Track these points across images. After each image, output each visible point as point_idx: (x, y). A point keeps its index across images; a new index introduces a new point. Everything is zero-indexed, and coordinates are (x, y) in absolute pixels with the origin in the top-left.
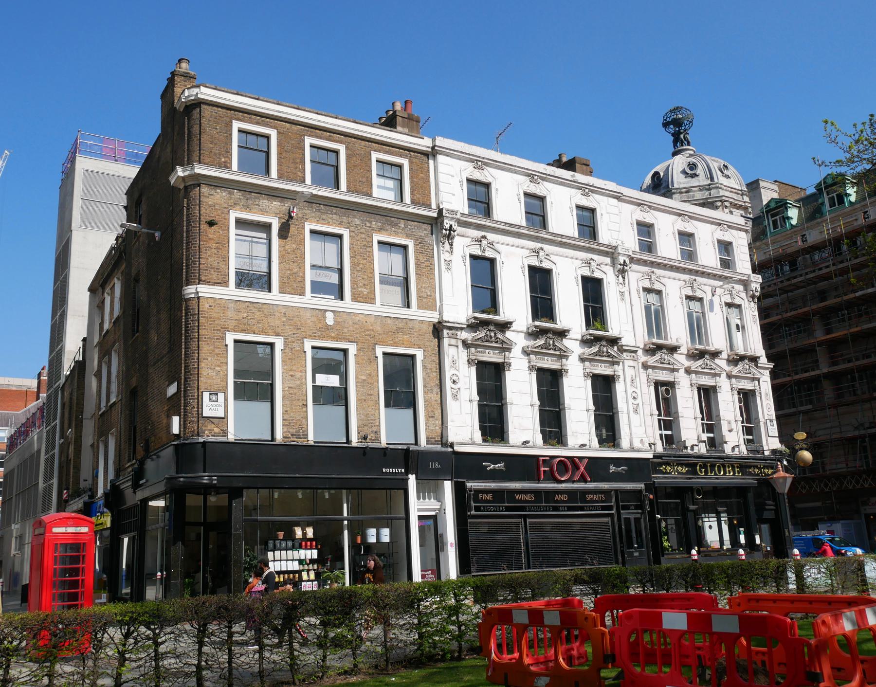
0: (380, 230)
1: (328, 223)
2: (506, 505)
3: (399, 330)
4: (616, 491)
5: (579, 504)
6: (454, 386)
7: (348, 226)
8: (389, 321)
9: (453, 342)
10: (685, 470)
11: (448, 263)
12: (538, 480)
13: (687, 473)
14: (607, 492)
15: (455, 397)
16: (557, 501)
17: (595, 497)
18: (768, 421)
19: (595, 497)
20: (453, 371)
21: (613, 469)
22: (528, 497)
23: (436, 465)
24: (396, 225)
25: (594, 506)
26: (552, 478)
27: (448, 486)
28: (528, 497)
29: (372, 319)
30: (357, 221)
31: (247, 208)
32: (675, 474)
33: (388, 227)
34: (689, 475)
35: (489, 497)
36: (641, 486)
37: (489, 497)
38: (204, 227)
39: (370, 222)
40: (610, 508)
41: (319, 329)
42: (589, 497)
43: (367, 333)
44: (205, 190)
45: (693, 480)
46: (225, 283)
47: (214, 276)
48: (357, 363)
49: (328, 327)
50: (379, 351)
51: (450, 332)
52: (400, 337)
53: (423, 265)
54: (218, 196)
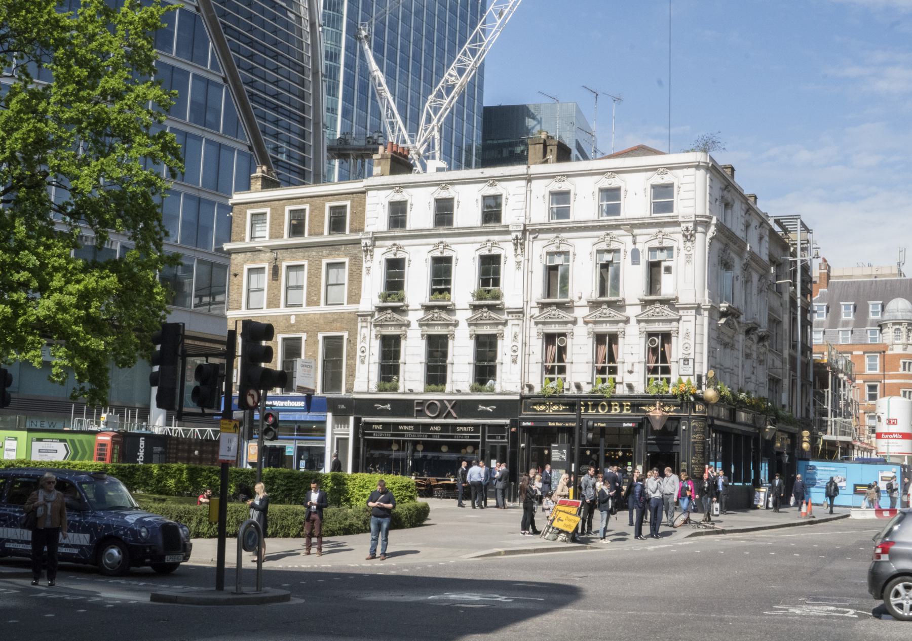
0: (328, 256)
1: (297, 259)
3: (334, 321)
4: (484, 425)
6: (362, 355)
7: (304, 258)
9: (364, 324)
10: (562, 408)
11: (368, 269)
12: (411, 416)
13: (564, 410)
14: (476, 426)
15: (363, 362)
16: (432, 431)
17: (464, 429)
18: (682, 362)
20: (363, 344)
21: (481, 407)
22: (409, 428)
23: (343, 407)
24: (339, 249)
26: (421, 413)
27: (352, 419)
28: (409, 428)
29: (318, 316)
30: (314, 253)
31: (253, 261)
33: (333, 253)
35: (380, 427)
36: (508, 421)
37: (380, 427)
38: (232, 277)
39: (322, 252)
40: (478, 437)
41: (287, 327)
42: (459, 429)
44: (233, 256)
45: (569, 417)
46: (239, 308)
47: (235, 305)
48: (307, 345)
49: (292, 325)
50: (320, 336)
51: (363, 318)
52: (334, 325)
53: (354, 274)
54: (239, 258)
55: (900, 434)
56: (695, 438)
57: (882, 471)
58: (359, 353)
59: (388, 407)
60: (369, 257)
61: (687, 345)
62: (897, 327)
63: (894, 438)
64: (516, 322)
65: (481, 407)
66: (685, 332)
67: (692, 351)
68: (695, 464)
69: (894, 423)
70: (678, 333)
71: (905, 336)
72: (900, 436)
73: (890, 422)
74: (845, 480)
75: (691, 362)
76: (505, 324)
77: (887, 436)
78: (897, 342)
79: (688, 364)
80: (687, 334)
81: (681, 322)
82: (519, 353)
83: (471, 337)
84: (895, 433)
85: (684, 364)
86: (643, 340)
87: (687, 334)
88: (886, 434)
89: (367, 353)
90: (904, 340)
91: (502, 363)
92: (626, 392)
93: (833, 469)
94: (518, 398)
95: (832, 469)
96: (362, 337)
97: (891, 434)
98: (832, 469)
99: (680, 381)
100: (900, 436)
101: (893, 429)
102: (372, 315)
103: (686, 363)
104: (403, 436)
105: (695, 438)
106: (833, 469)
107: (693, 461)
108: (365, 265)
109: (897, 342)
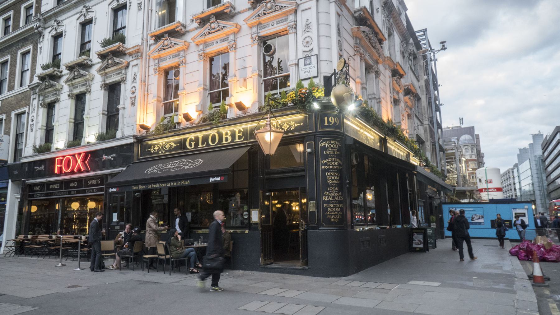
2: (45, 192)
3: (22, 99)
5: (83, 189)
8: (19, 96)
9: (34, 96)
15: (32, 130)
17: (93, 182)
18: (302, 62)
19: (93, 182)
21: (105, 157)
25: (92, 189)
29: (13, 98)
32: (162, 152)
34: (178, 150)
43: (11, 106)
55: (495, 188)
56: (326, 164)
57: (515, 209)
58: (30, 123)
59: (42, 168)
60: (41, 38)
61: (307, 39)
62: (466, 147)
63: (491, 191)
64: (135, 62)
65: (105, 157)
66: (304, 23)
67: (315, 46)
68: (328, 202)
69: (490, 182)
70: (296, 28)
71: (470, 151)
72: (495, 190)
73: (488, 182)
74: (482, 217)
75: (314, 59)
76: (127, 67)
77: (487, 190)
78: (466, 154)
79: (310, 63)
80: (308, 26)
81: (299, 13)
82: (138, 94)
83: (101, 87)
84: (492, 188)
85: (305, 65)
86: (256, 47)
87: (308, 26)
88: (486, 189)
89: (34, 122)
90: (470, 153)
91: (124, 108)
92: (240, 113)
93: (472, 209)
94: (132, 140)
95: (470, 209)
96: (33, 107)
97: (490, 189)
98: (470, 209)
99: (300, 86)
100: (495, 190)
101: (490, 186)
102: (37, 86)
103: (308, 62)
104: (51, 194)
105: (326, 164)
106: (472, 209)
107: (325, 198)
108: (39, 46)
109: (466, 154)
